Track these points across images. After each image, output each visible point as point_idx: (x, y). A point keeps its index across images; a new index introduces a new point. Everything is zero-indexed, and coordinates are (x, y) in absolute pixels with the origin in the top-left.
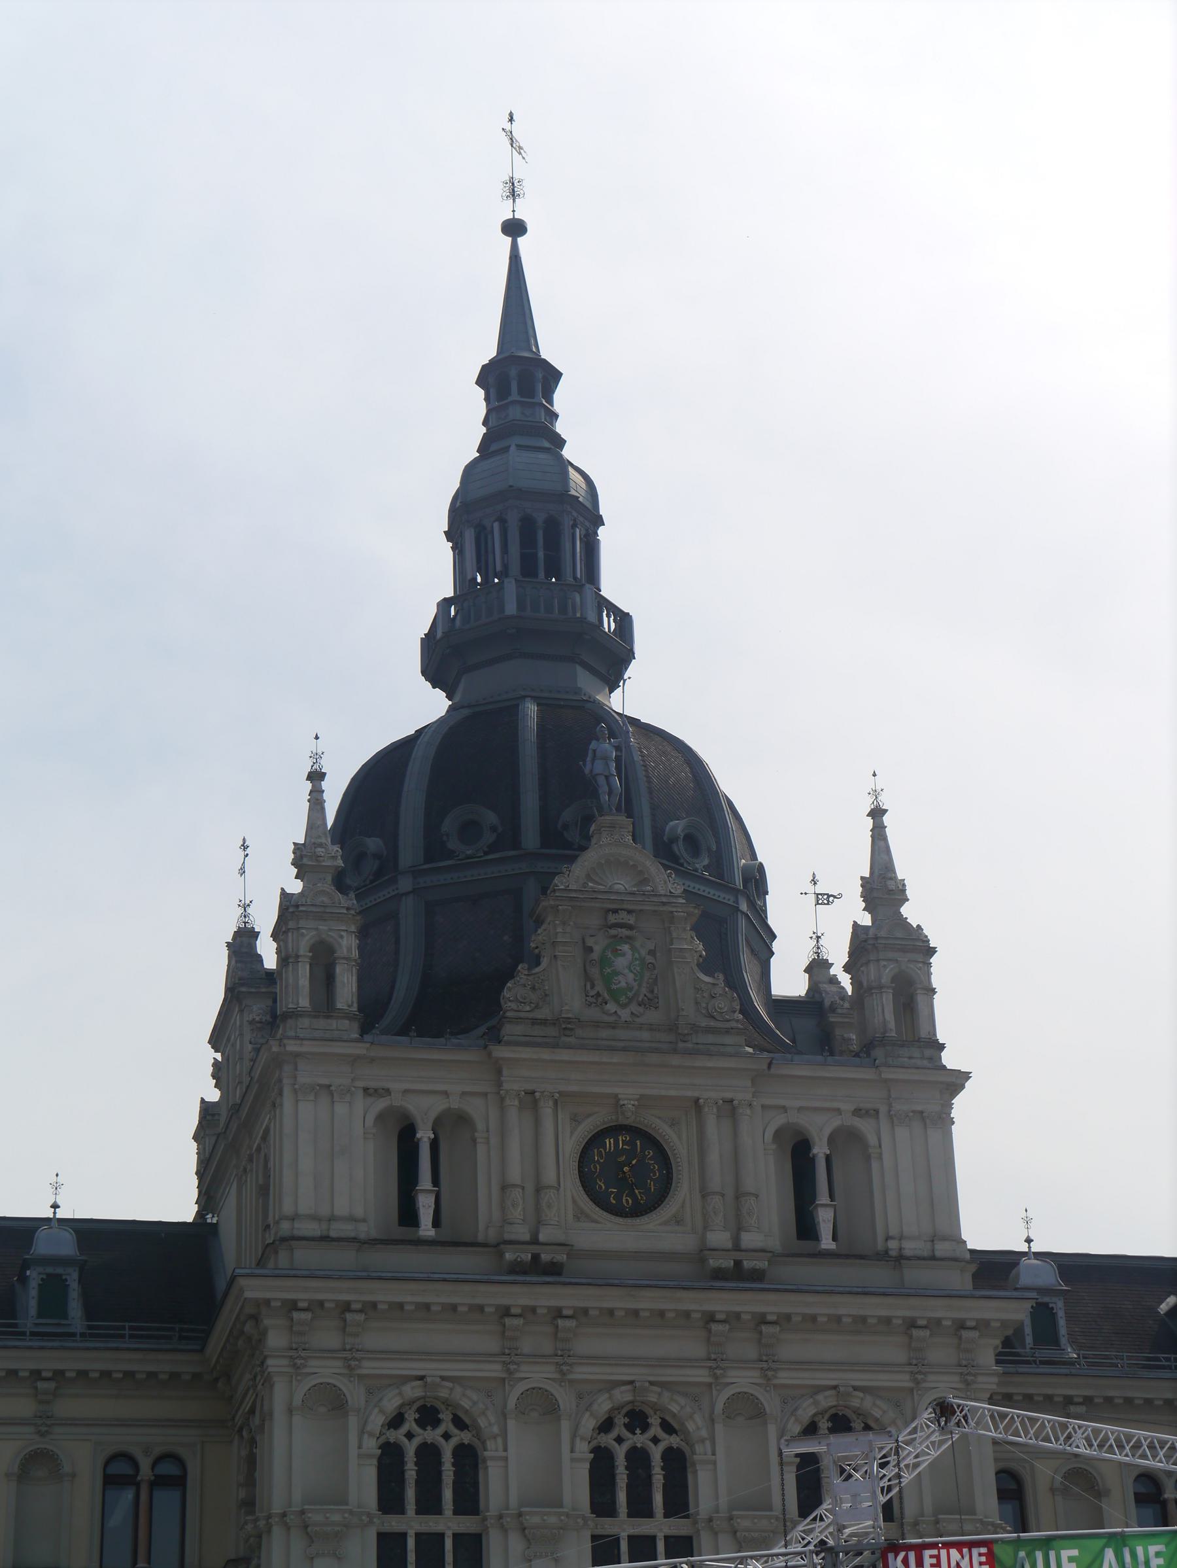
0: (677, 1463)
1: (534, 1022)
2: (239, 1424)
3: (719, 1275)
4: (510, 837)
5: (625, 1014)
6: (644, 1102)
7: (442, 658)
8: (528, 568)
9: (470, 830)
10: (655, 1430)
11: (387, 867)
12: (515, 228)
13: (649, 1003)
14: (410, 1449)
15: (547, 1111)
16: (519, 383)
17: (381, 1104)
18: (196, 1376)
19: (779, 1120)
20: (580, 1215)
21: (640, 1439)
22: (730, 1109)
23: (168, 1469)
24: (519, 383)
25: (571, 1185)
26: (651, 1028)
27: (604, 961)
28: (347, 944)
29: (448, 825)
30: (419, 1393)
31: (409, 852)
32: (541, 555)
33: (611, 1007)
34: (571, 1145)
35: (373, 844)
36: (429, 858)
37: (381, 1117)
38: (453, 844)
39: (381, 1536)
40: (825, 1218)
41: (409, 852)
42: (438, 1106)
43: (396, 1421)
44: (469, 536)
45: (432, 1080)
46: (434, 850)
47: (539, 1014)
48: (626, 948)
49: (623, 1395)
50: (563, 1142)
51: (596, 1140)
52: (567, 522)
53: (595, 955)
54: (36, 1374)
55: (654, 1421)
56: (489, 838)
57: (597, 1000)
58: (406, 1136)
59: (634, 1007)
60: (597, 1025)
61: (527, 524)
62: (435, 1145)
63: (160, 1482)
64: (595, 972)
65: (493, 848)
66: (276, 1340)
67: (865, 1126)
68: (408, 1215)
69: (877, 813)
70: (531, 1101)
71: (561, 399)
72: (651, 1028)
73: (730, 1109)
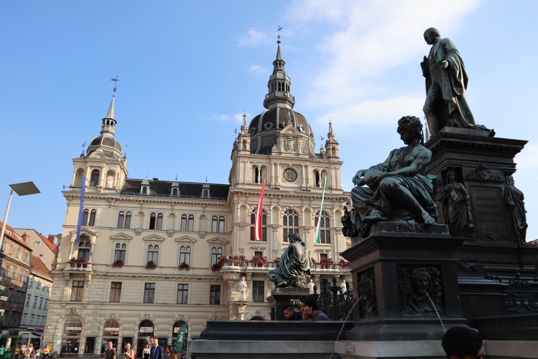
0: (297, 218)
2: (231, 211)
3: (304, 190)
4: (274, 127)
7: (267, 103)
8: (279, 89)
10: (293, 213)
12: (279, 42)
16: (278, 64)
17: (253, 164)
19: (313, 168)
21: (291, 215)
22: (306, 166)
23: (222, 218)
24: (278, 64)
28: (248, 140)
29: (265, 125)
31: (260, 129)
35: (254, 129)
37: (253, 166)
38: (266, 128)
40: (320, 183)
41: (260, 129)
42: (262, 164)
44: (271, 85)
45: (260, 161)
46: (263, 129)
50: (280, 171)
54: (202, 204)
55: (293, 212)
61: (279, 83)
63: (220, 220)
66: (235, 199)
67: (327, 169)
68: (257, 181)
69: (330, 124)
70: (275, 164)
73: (306, 166)
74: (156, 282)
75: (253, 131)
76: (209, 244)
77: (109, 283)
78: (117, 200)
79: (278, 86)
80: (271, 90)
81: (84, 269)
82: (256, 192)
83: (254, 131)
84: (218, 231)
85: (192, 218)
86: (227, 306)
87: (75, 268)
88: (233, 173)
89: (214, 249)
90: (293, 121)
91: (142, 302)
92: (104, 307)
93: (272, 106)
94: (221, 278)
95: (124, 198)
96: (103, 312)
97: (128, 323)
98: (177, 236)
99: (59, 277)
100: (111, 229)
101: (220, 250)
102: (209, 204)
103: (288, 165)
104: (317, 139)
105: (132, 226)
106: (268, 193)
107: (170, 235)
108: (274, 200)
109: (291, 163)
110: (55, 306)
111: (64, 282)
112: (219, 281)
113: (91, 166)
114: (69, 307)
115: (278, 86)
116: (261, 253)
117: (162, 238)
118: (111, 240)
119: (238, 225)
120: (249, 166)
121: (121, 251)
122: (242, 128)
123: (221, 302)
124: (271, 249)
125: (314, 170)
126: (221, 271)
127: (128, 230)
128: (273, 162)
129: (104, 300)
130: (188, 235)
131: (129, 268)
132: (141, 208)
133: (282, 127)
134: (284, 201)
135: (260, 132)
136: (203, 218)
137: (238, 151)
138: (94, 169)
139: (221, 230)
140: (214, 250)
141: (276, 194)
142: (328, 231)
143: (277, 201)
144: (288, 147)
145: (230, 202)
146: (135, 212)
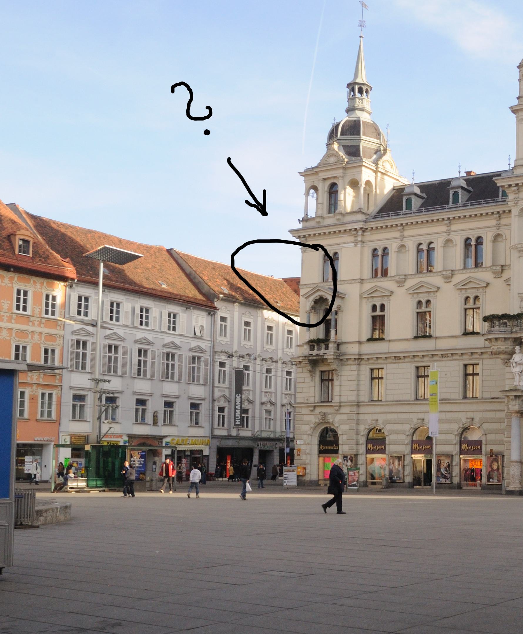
54: (493, 213)
74: (431, 364)
77: (365, 370)
78: (364, 230)
81: (326, 352)
85: (479, 241)
87: (315, 352)
91: (413, 397)
92: (362, 410)
95: (373, 225)
96: (361, 417)
97: (396, 432)
98: (458, 278)
99: (302, 367)
100: (362, 281)
105: (392, 272)
107: (448, 278)
110: (305, 411)
111: (308, 374)
113: (325, 179)
114: (318, 410)
117: (434, 286)
118: (364, 301)
121: (380, 316)
127: (385, 279)
129: (362, 399)
130: (472, 275)
131: (392, 344)
132: (402, 238)
136: (500, 239)
138: (328, 183)
146: (393, 248)
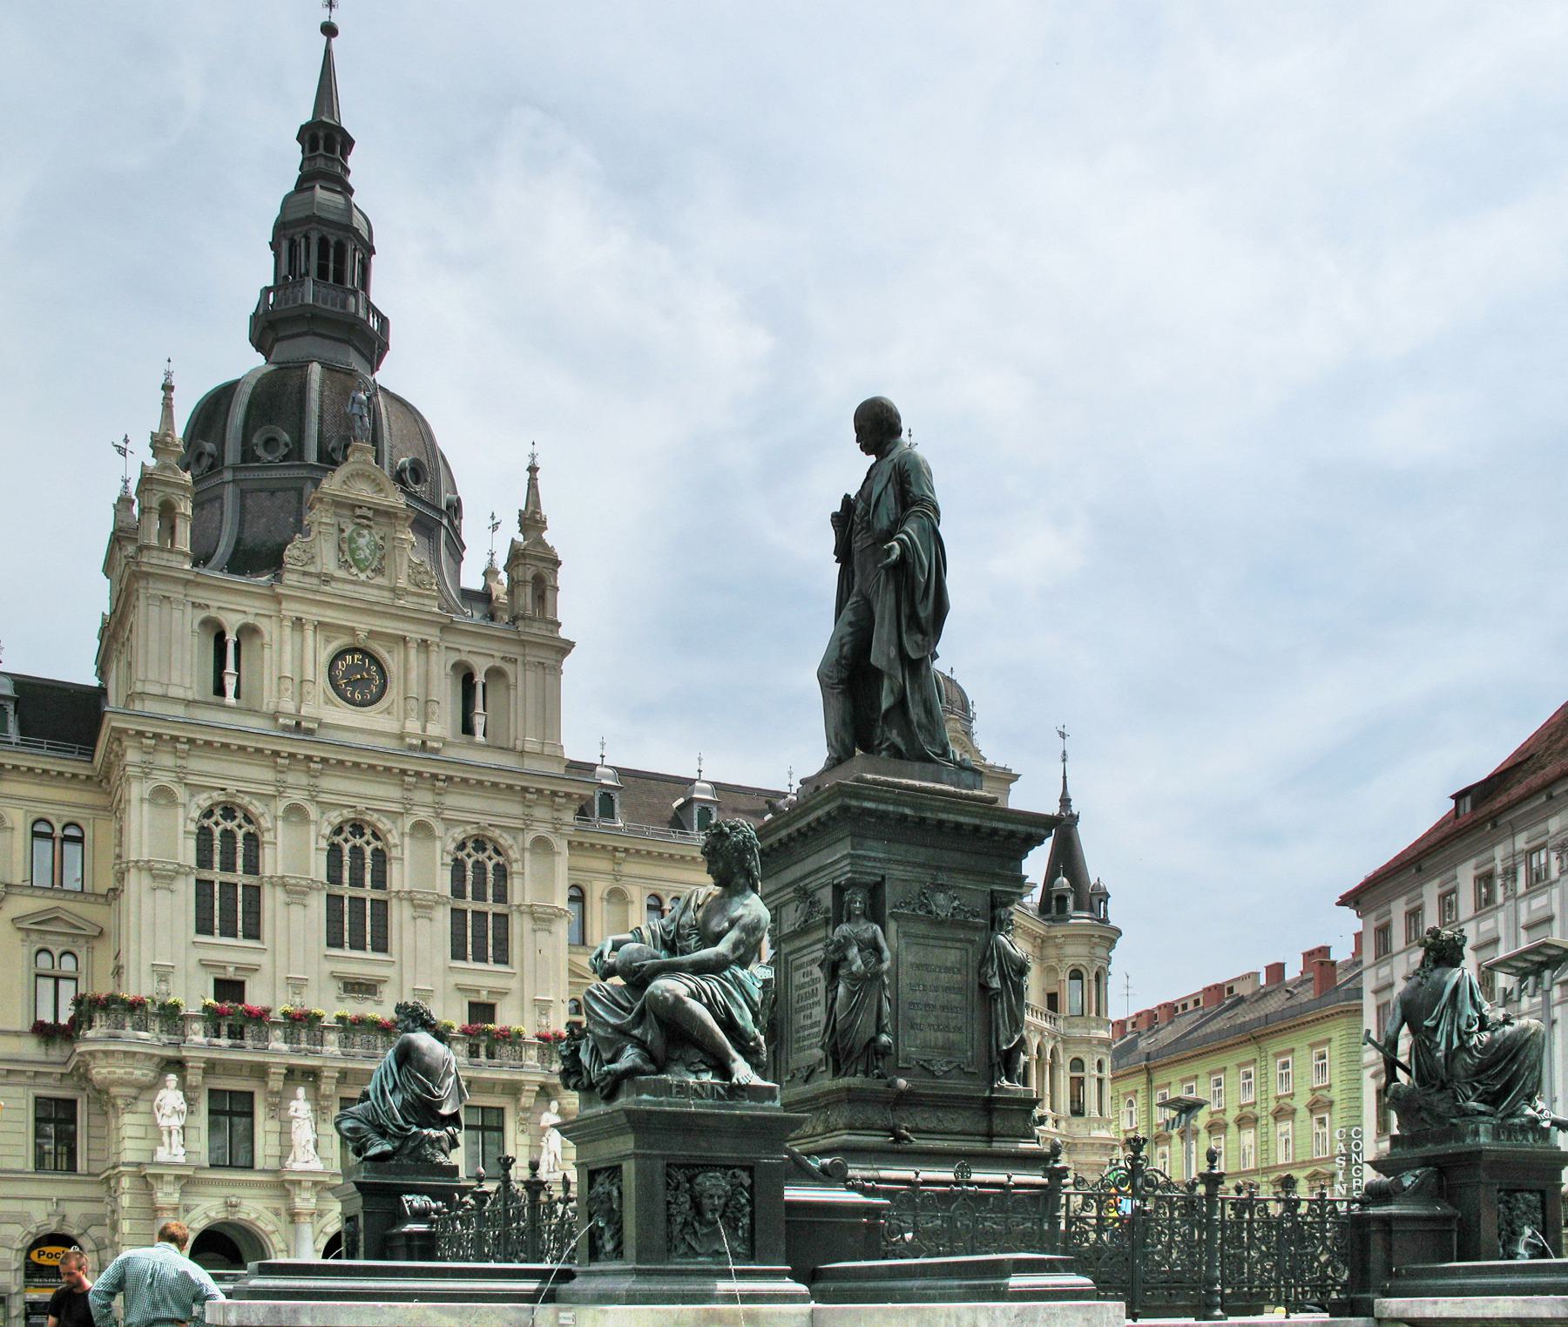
1: (305, 574)
2: (114, 809)
5: (363, 577)
6: (371, 632)
8: (322, 273)
9: (270, 442)
11: (216, 464)
13: (379, 571)
14: (217, 831)
15: (309, 633)
18: (88, 777)
20: (328, 701)
25: (323, 681)
26: (380, 587)
27: (351, 540)
30: (223, 798)
31: (232, 455)
32: (331, 266)
33: (354, 570)
34: (325, 655)
35: (209, 447)
36: (244, 460)
38: (260, 452)
39: (198, 881)
41: (232, 455)
43: (209, 814)
44: (285, 245)
46: (248, 455)
47: (311, 569)
48: (365, 532)
49: (348, 814)
51: (339, 655)
52: (350, 247)
53: (346, 535)
56: (283, 451)
57: (344, 565)
58: (220, 639)
59: (369, 573)
60: (345, 581)
61: (323, 242)
62: (238, 646)
63: (67, 839)
64: (345, 547)
65: (285, 458)
68: (220, 690)
70: (298, 623)
71: (352, 161)
72: (380, 587)
75: (201, 455)
76: (20, 935)
79: (321, 256)
80: (284, 271)
82: (218, 739)
83: (206, 462)
84: (56, 885)
86: (108, 1182)
88: (114, 634)
89: (44, 957)
90: (375, 439)
93: (287, 351)
94: (81, 1075)
101: (68, 964)
102: (15, 767)
103: (352, 631)
104: (472, 528)
106: (269, 746)
108: (291, 778)
109: (363, 624)
112: (68, 1082)
115: (321, 256)
116: (240, 985)
119: (148, 868)
120: (186, 622)
122: (159, 444)
123: (81, 1164)
124: (281, 975)
125: (456, 666)
126: (82, 1048)
128: (291, 609)
133: (329, 460)
134: (333, 783)
135: (235, 469)
137: (141, 549)
139: (71, 883)
140: (44, 960)
141: (298, 749)
142: (502, 920)
143: (304, 780)
144: (352, 552)
145: (109, 766)
